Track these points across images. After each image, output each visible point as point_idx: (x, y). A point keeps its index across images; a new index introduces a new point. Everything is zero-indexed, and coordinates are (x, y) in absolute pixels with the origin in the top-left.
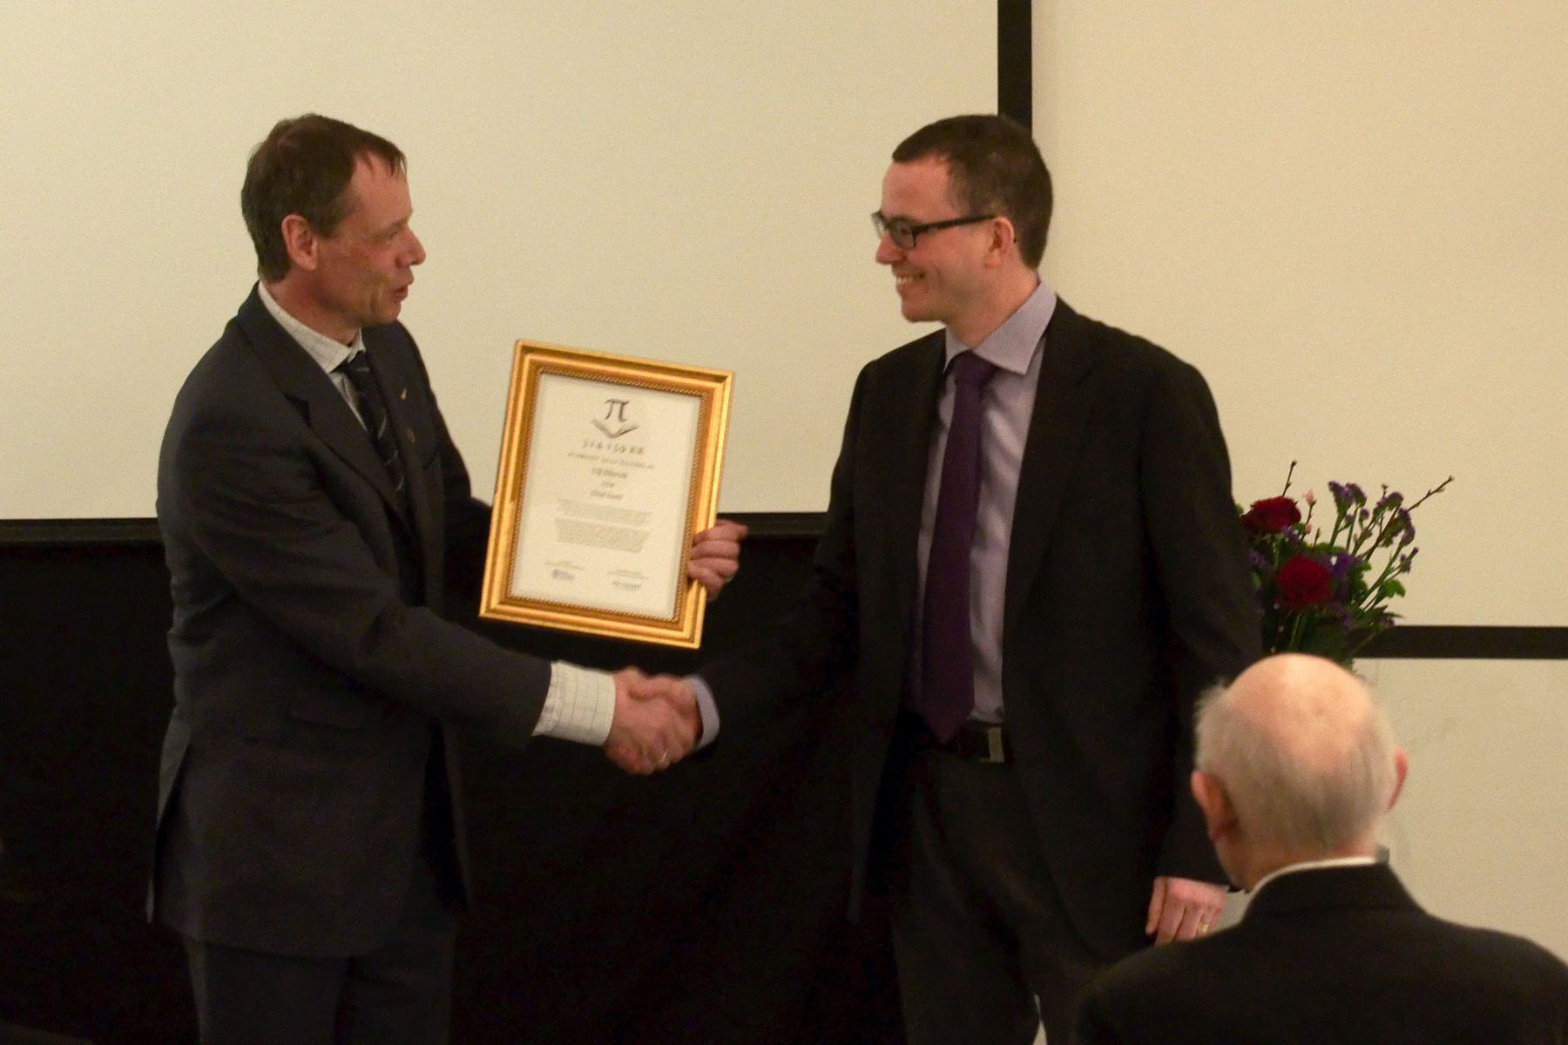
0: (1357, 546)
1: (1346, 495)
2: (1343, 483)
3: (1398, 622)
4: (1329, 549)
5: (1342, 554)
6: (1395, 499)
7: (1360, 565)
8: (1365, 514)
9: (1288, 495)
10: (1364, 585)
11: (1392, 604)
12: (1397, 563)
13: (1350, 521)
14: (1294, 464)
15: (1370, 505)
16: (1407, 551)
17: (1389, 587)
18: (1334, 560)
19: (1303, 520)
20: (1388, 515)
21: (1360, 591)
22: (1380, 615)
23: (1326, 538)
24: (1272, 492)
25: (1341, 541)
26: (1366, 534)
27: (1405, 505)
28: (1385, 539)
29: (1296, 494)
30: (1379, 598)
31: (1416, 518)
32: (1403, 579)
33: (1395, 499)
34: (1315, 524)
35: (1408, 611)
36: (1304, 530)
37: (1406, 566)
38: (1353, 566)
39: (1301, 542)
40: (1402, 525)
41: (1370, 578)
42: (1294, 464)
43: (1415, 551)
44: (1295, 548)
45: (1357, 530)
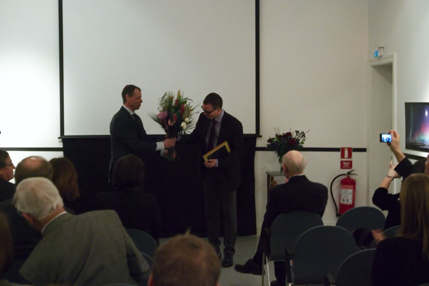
0: (298, 138)
1: (297, 132)
2: (297, 130)
3: (303, 147)
4: (295, 138)
5: (297, 139)
6: (303, 132)
7: (299, 140)
8: (299, 134)
9: (290, 132)
10: (299, 143)
11: (303, 145)
12: (303, 140)
13: (298, 135)
14: (291, 128)
15: (300, 133)
16: (304, 138)
17: (302, 143)
18: (296, 140)
19: (292, 135)
20: (302, 134)
21: (299, 143)
22: (301, 146)
23: (295, 137)
24: (288, 131)
25: (297, 137)
26: (299, 137)
27: (304, 133)
28: (302, 137)
29: (291, 132)
30: (301, 144)
31: (306, 135)
32: (304, 142)
33: (303, 132)
34: (294, 135)
35: (305, 145)
36: (292, 136)
37: (304, 140)
38: (298, 140)
39: (292, 138)
40: (304, 135)
41: (300, 142)
42: (291, 128)
43: (305, 139)
44: (291, 138)
45: (298, 136)
